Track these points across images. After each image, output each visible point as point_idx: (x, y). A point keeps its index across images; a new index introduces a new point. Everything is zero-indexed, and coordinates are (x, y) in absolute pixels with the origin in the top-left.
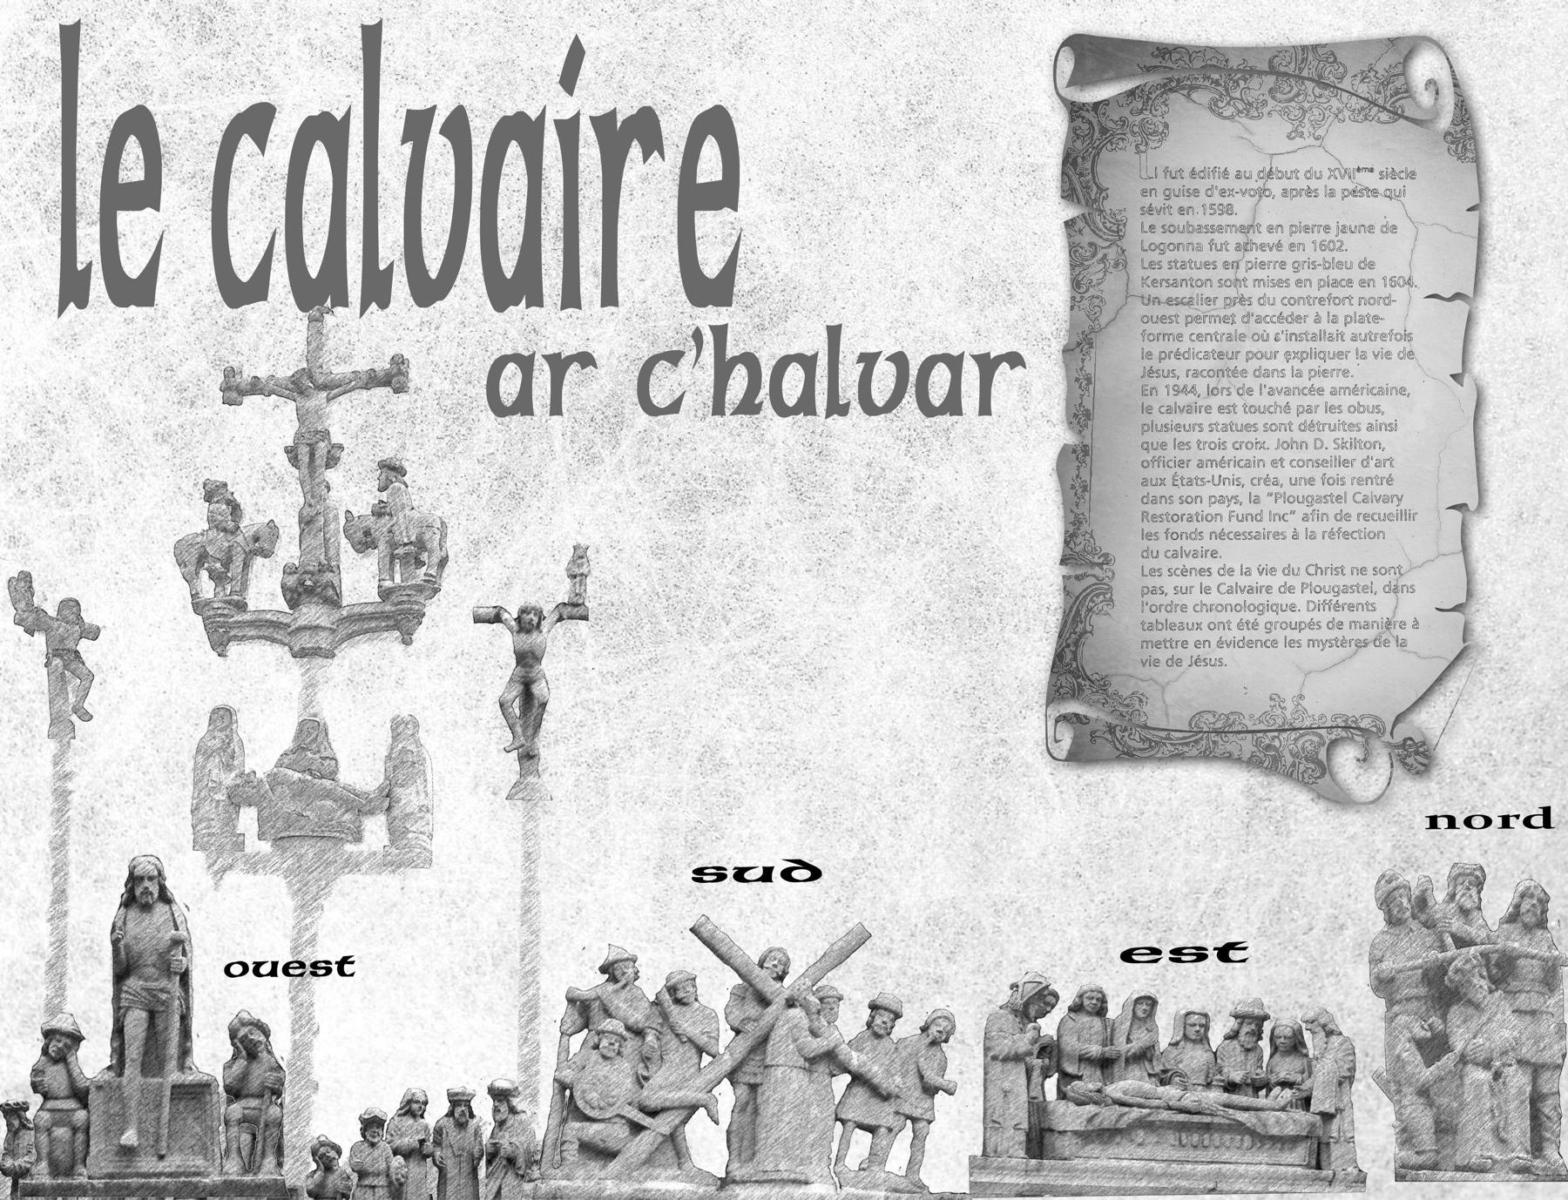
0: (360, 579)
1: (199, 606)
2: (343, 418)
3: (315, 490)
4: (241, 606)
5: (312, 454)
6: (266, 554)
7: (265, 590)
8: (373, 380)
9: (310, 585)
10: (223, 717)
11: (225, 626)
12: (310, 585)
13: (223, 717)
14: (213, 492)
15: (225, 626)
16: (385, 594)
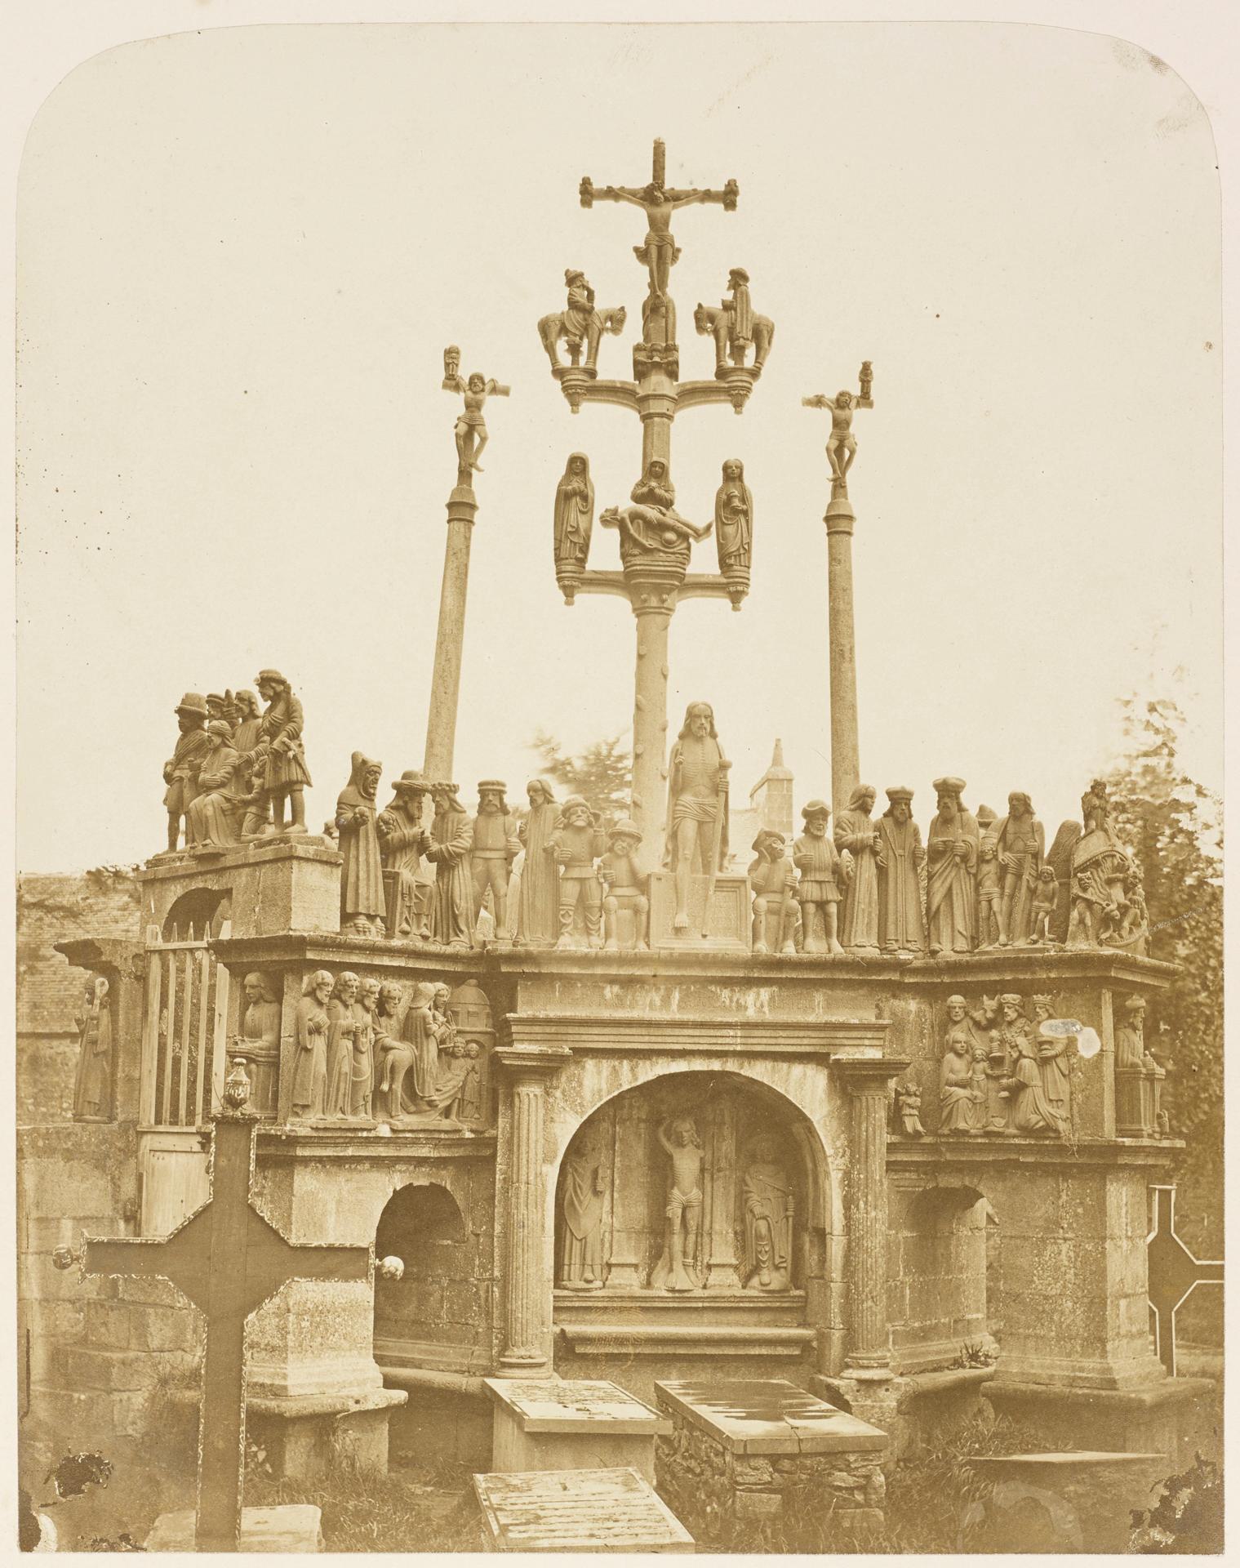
0: (697, 357)
1: (559, 373)
2: (683, 222)
3: (658, 281)
4: (592, 374)
5: (658, 253)
6: (616, 330)
7: (615, 359)
8: (707, 196)
9: (657, 358)
10: (578, 466)
11: (581, 387)
12: (657, 358)
13: (578, 466)
14: (573, 279)
15: (581, 387)
16: (721, 373)
